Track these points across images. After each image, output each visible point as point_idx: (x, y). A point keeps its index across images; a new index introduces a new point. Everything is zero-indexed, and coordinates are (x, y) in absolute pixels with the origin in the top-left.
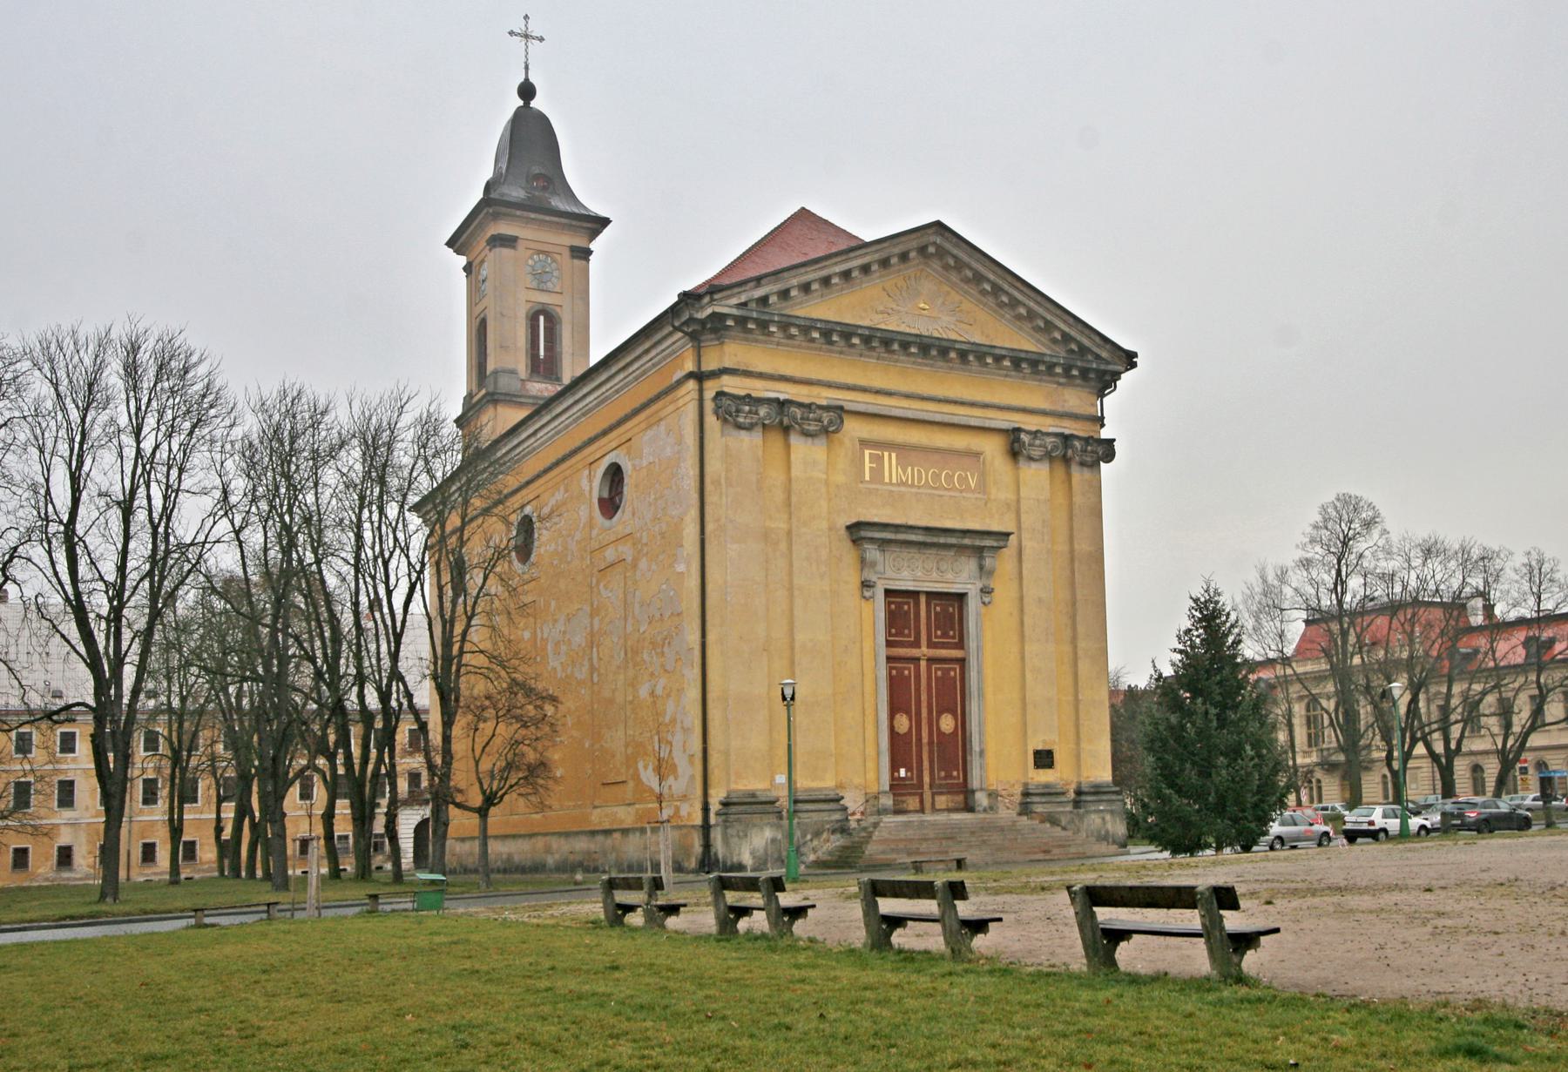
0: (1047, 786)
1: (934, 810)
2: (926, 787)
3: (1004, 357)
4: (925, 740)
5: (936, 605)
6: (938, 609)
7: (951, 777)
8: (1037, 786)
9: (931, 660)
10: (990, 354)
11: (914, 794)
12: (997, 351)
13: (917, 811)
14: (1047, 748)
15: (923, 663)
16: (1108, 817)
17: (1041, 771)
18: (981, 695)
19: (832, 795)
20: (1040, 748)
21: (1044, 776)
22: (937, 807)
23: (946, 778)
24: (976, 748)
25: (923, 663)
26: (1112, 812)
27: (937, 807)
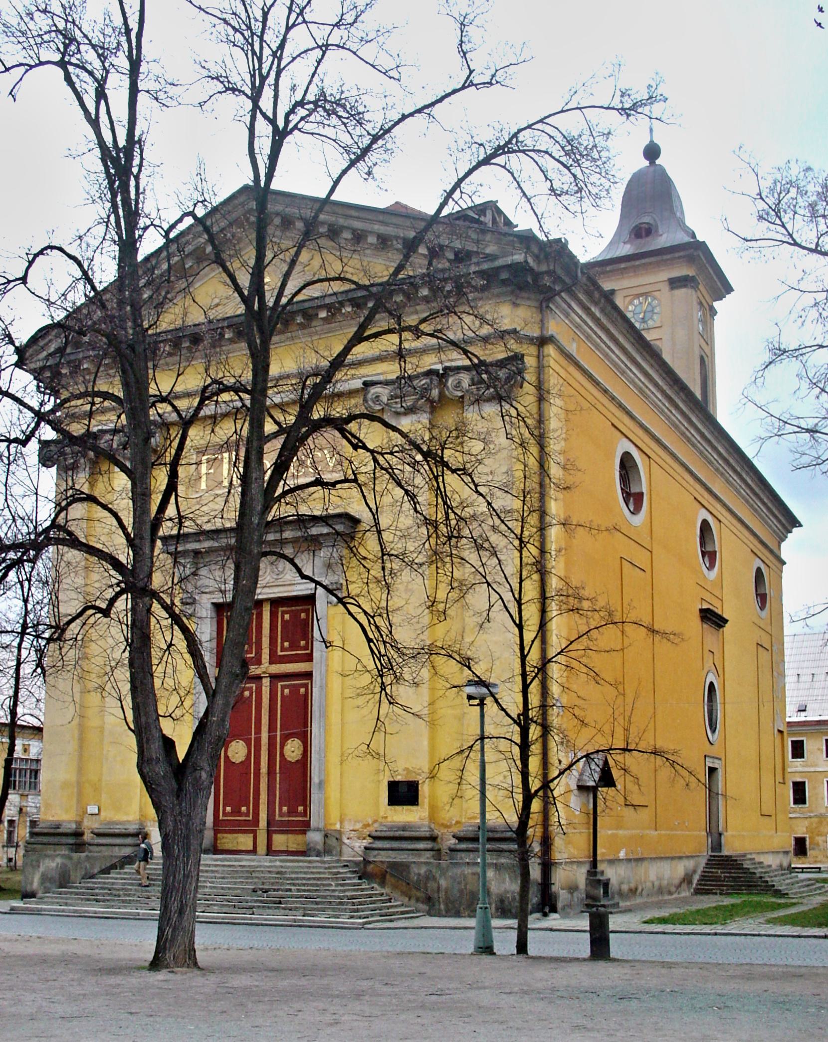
0: (404, 828)
1: (270, 851)
2: (263, 823)
3: (342, 304)
4: (264, 769)
5: (283, 613)
6: (287, 617)
7: (239, 813)
8: (391, 829)
9: (275, 678)
10: (320, 307)
11: (245, 832)
12: (328, 301)
13: (247, 852)
14: (411, 778)
15: (266, 682)
16: (490, 874)
17: (398, 808)
18: (324, 715)
19: (133, 828)
20: (399, 778)
21: (404, 815)
22: (251, 848)
23: (233, 813)
24: (315, 779)
25: (266, 682)
26: (497, 867)
27: (251, 848)
